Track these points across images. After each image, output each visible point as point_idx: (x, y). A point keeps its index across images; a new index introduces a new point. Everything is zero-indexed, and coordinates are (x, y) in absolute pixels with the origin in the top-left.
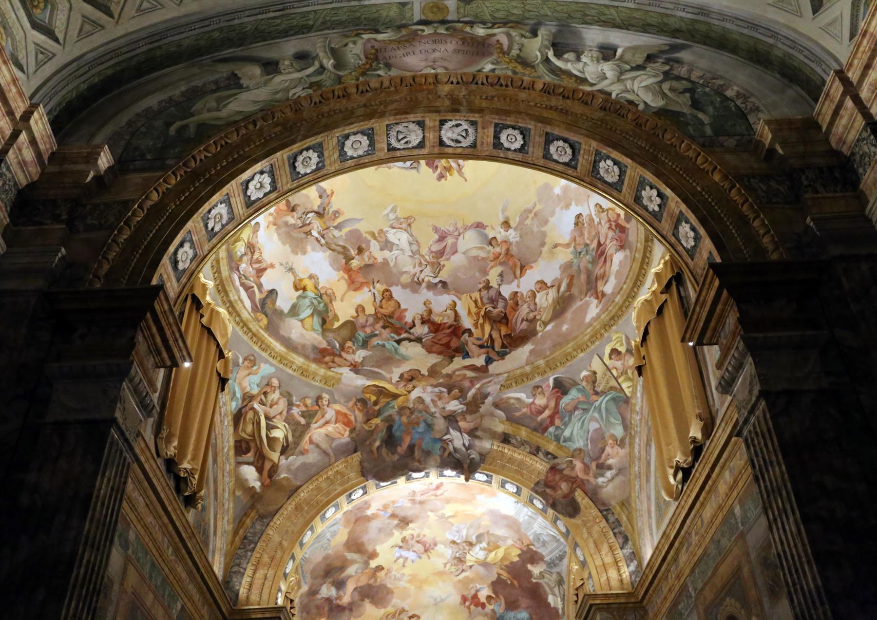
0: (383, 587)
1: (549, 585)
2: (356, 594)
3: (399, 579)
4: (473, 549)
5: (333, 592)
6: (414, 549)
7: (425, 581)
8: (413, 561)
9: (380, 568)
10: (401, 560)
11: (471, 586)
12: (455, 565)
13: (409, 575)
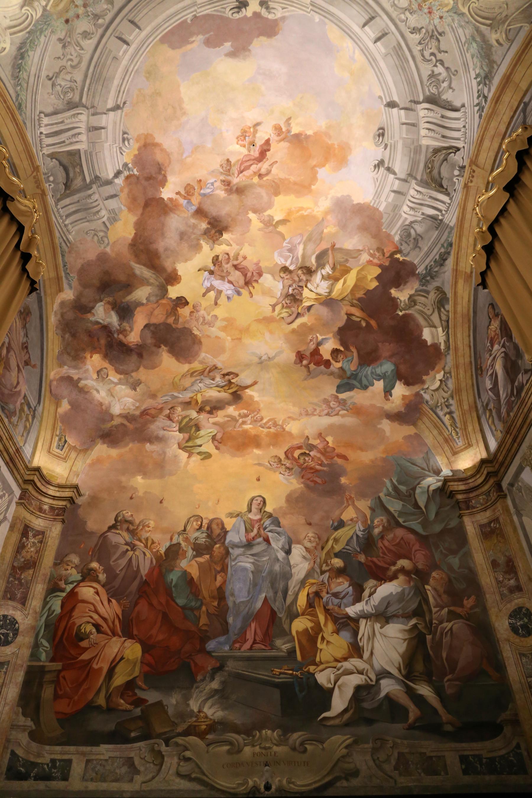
0: (187, 332)
1: (421, 313)
2: (148, 334)
3: (210, 324)
4: (313, 277)
5: (113, 319)
6: (231, 278)
7: (246, 330)
8: (228, 298)
9: (182, 302)
10: (212, 294)
11: (310, 338)
12: (288, 307)
13: (224, 319)
